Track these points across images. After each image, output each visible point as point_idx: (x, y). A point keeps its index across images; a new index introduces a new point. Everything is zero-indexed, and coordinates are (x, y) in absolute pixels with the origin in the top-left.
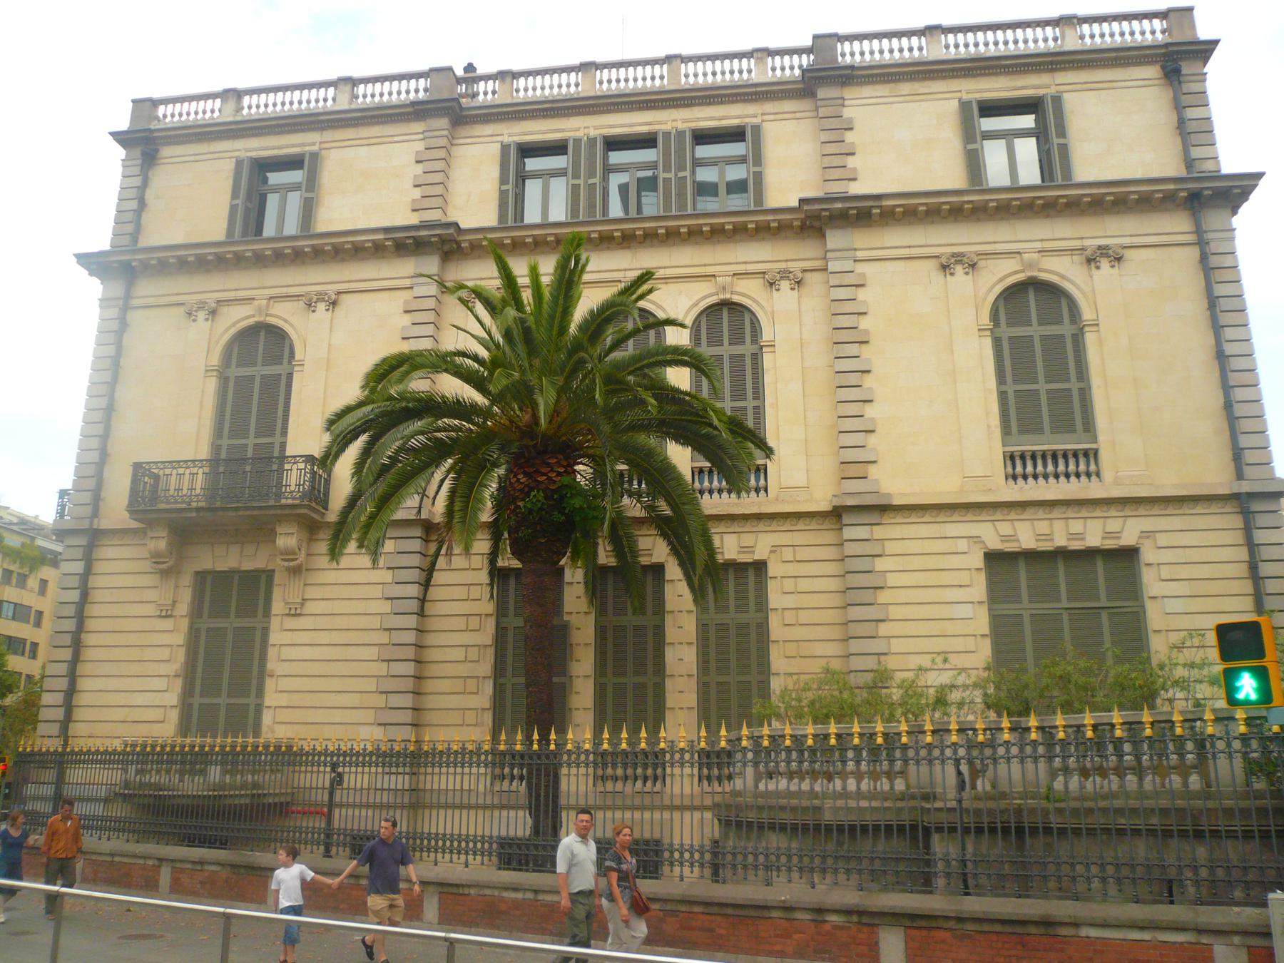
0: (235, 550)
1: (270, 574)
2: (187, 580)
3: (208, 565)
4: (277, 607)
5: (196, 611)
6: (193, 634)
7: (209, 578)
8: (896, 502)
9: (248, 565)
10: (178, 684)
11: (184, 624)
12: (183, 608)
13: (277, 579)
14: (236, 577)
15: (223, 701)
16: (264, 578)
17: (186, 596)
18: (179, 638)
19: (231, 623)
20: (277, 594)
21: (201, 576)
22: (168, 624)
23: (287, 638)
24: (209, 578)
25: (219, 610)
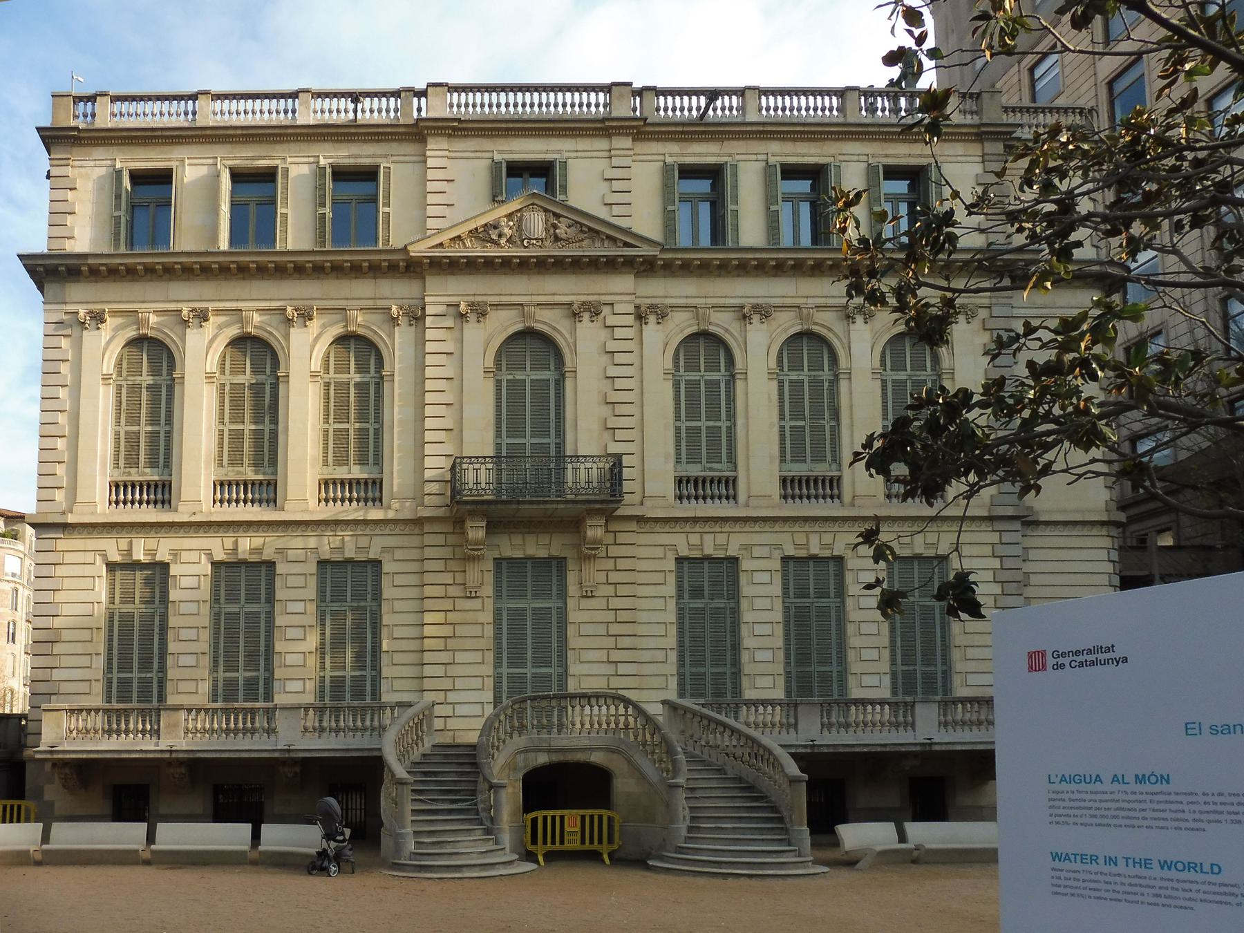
0: (531, 539)
1: (561, 562)
2: (490, 565)
3: (508, 552)
4: (572, 589)
5: (498, 595)
6: (497, 613)
7: (504, 564)
8: (1042, 519)
9: (542, 553)
10: (490, 656)
11: (489, 604)
12: (488, 590)
13: (571, 565)
14: (529, 563)
15: (529, 671)
16: (554, 563)
17: (489, 578)
18: (488, 617)
19: (530, 604)
20: (572, 578)
21: (498, 562)
22: (475, 604)
23: (584, 616)
24: (504, 564)
25: (517, 592)
